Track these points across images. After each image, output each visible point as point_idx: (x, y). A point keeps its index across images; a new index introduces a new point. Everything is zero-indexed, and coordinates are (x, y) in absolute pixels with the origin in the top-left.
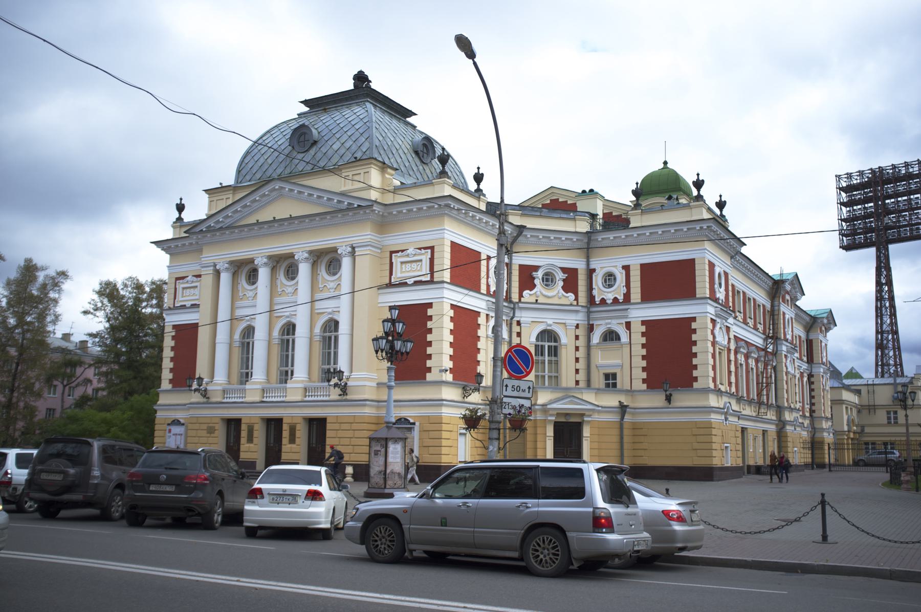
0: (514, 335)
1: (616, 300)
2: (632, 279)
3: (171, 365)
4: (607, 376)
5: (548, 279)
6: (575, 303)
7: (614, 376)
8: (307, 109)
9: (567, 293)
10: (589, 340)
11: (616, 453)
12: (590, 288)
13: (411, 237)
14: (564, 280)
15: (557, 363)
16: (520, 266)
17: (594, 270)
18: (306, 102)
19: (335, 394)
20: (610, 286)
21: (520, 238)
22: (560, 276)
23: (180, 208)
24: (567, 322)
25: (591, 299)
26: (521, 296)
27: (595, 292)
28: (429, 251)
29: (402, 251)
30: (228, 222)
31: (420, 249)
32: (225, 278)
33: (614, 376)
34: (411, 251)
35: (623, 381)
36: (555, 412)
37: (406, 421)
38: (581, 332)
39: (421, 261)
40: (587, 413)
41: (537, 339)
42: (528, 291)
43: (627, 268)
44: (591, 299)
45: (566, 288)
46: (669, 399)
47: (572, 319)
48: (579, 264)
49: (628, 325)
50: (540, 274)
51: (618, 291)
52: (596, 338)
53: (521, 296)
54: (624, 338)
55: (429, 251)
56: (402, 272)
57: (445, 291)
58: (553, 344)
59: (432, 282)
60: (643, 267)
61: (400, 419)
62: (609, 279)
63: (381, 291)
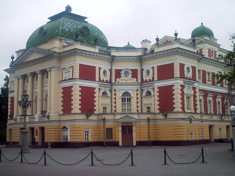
0: (113, 95)
2: (155, 72)
5: (126, 73)
6: (136, 82)
8: (50, 20)
10: (142, 95)
11: (147, 136)
13: (67, 63)
14: (132, 74)
15: (130, 104)
16: (115, 70)
18: (49, 18)
19: (46, 120)
21: (114, 60)
22: (130, 72)
23: (13, 58)
24: (133, 89)
26: (116, 80)
27: (144, 77)
29: (65, 68)
30: (21, 62)
31: (69, 67)
35: (152, 110)
36: (121, 122)
38: (139, 92)
39: (70, 71)
40: (133, 122)
41: (122, 96)
42: (118, 79)
43: (153, 68)
45: (133, 77)
46: (166, 116)
47: (135, 88)
48: (139, 68)
49: (154, 88)
50: (123, 72)
52: (144, 94)
53: (116, 80)
54: (152, 94)
55: (72, 68)
57: (76, 81)
58: (129, 97)
60: (158, 67)
63: (60, 83)
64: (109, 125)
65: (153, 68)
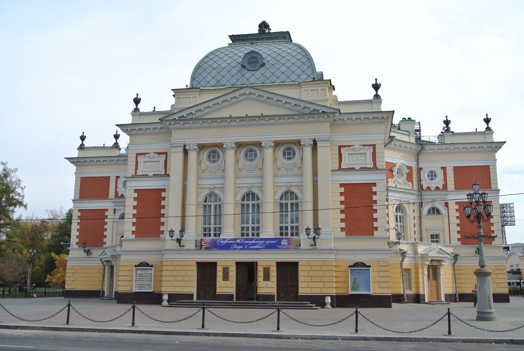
1: (437, 188)
4: (432, 236)
7: (437, 236)
9: (408, 181)
10: (420, 212)
12: (419, 180)
14: (407, 174)
17: (421, 169)
20: (432, 179)
25: (421, 187)
28: (165, 155)
29: (349, 146)
30: (198, 114)
31: (364, 146)
32: (193, 156)
33: (437, 236)
34: (357, 146)
37: (363, 265)
39: (365, 154)
40: (444, 260)
43: (444, 169)
44: (421, 187)
48: (413, 165)
49: (447, 204)
51: (439, 182)
56: (144, 168)
59: (375, 168)
60: (455, 168)
62: (432, 175)
64: (407, 263)
65: (444, 169)
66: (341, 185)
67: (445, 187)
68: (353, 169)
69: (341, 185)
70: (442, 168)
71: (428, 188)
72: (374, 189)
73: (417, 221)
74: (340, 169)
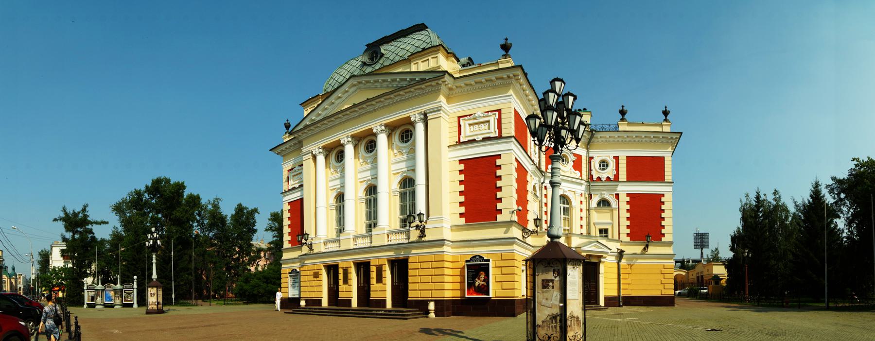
1: (608, 178)
3: (289, 215)
4: (601, 231)
7: (606, 231)
17: (592, 158)
20: (603, 169)
27: (592, 173)
33: (606, 231)
39: (488, 122)
49: (617, 196)
51: (610, 172)
54: (614, 204)
58: (566, 206)
59: (500, 137)
61: (475, 257)
66: (461, 162)
67: (617, 177)
68: (474, 141)
69: (461, 162)
70: (614, 157)
71: (599, 179)
72: (498, 162)
73: (584, 214)
74: (459, 143)
